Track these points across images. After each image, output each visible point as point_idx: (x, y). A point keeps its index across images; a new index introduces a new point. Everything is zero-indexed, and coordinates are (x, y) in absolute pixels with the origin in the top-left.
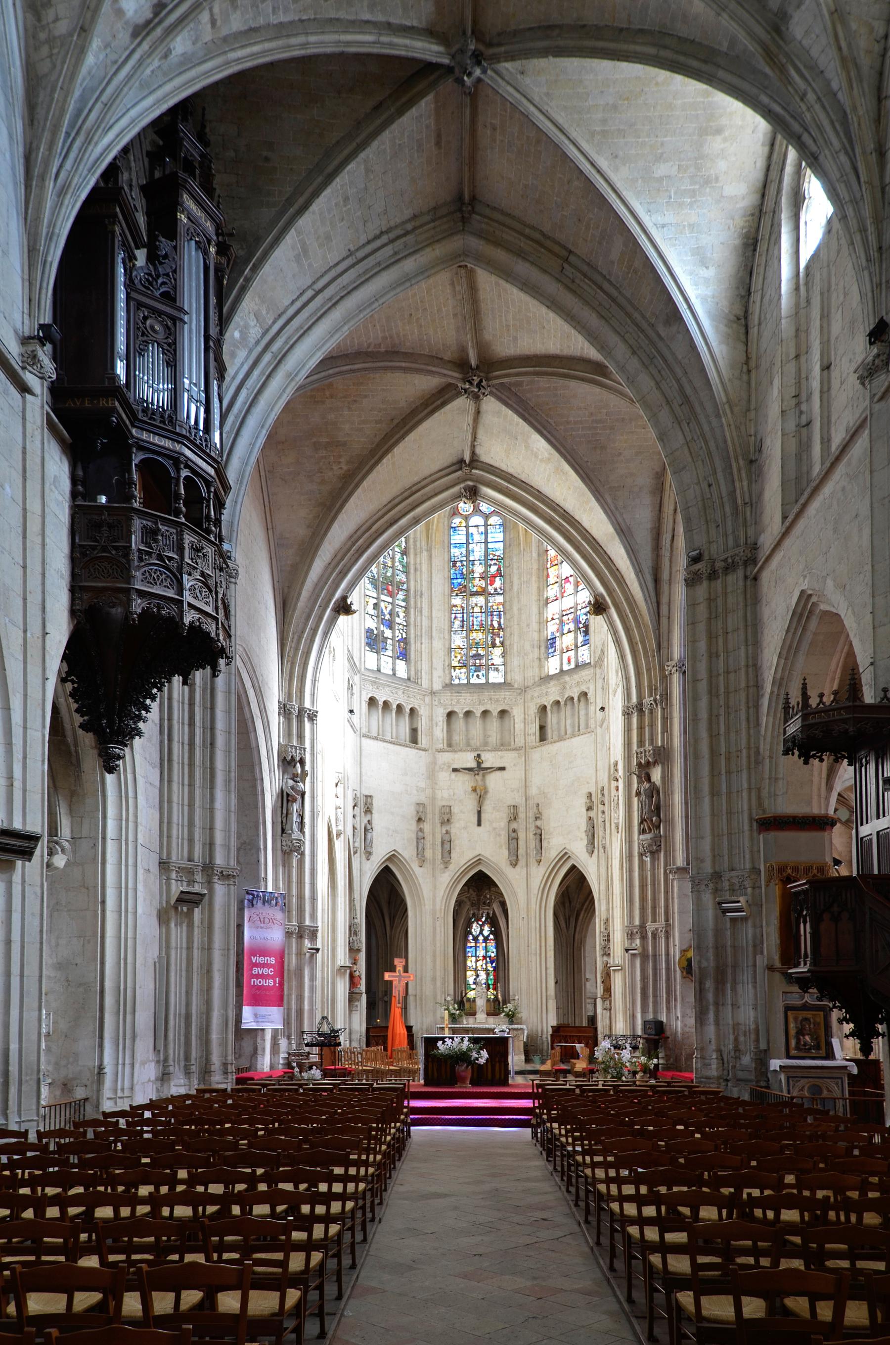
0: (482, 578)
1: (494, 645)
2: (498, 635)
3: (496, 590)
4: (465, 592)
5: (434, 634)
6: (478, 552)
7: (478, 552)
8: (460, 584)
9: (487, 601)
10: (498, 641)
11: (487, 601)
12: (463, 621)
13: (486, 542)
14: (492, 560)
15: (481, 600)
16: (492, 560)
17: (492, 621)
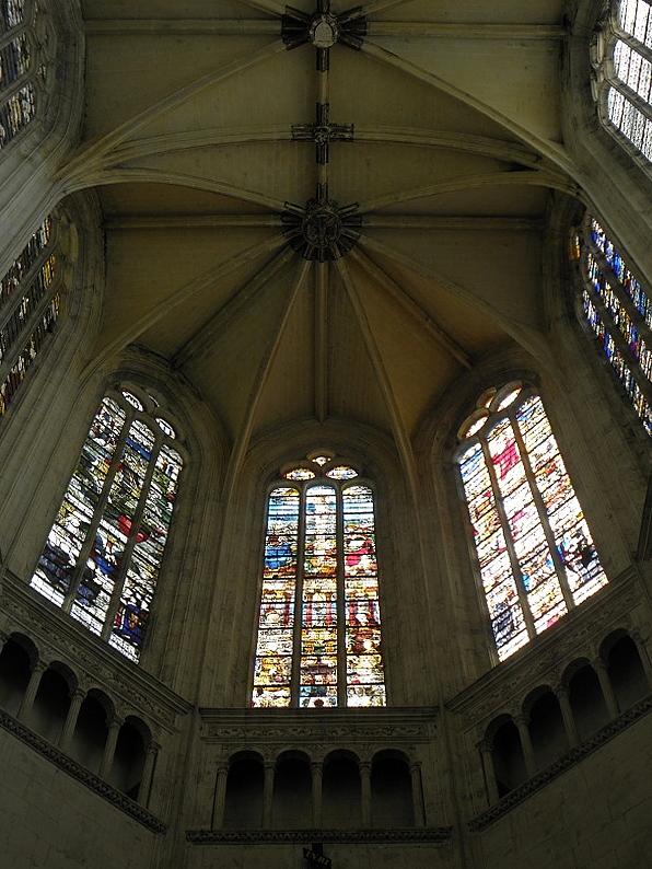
0: (332, 556)
1: (359, 651)
2: (370, 635)
3: (361, 571)
4: (291, 574)
5: (215, 613)
6: (322, 524)
7: (322, 524)
8: (283, 564)
9: (341, 588)
10: (367, 645)
11: (341, 588)
12: (286, 614)
13: (340, 514)
14: (352, 533)
15: (331, 585)
16: (352, 533)
17: (354, 614)
